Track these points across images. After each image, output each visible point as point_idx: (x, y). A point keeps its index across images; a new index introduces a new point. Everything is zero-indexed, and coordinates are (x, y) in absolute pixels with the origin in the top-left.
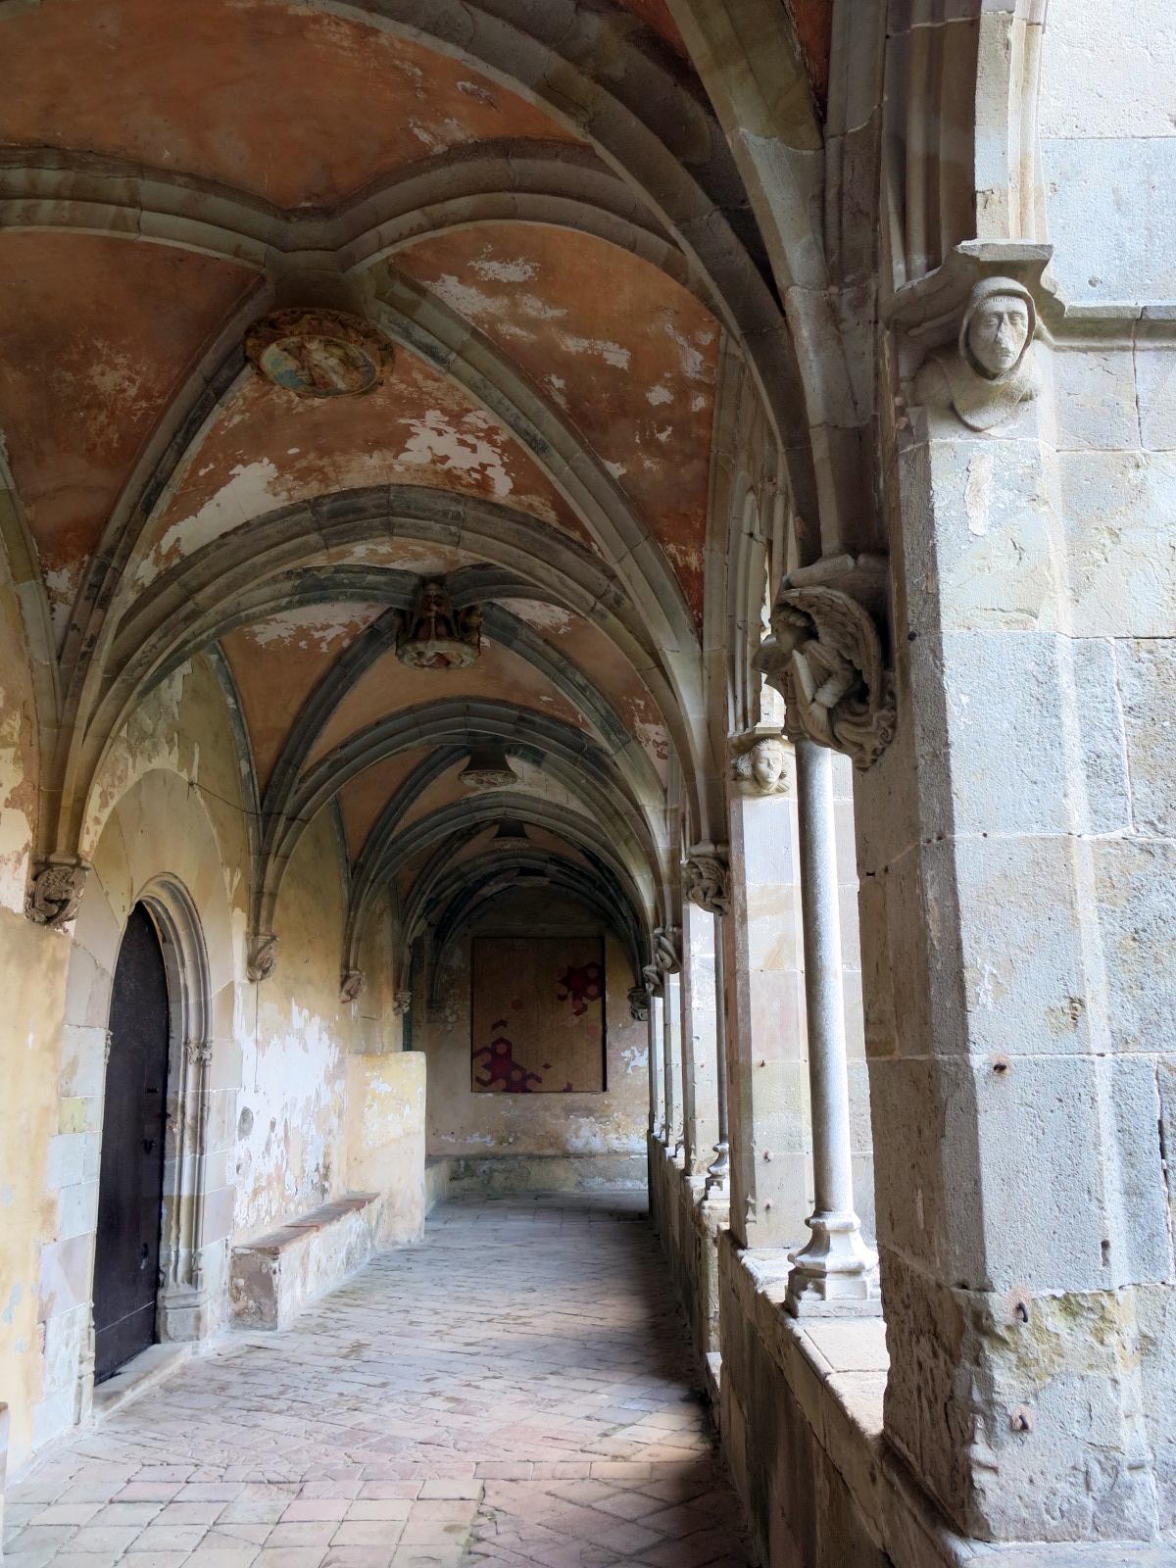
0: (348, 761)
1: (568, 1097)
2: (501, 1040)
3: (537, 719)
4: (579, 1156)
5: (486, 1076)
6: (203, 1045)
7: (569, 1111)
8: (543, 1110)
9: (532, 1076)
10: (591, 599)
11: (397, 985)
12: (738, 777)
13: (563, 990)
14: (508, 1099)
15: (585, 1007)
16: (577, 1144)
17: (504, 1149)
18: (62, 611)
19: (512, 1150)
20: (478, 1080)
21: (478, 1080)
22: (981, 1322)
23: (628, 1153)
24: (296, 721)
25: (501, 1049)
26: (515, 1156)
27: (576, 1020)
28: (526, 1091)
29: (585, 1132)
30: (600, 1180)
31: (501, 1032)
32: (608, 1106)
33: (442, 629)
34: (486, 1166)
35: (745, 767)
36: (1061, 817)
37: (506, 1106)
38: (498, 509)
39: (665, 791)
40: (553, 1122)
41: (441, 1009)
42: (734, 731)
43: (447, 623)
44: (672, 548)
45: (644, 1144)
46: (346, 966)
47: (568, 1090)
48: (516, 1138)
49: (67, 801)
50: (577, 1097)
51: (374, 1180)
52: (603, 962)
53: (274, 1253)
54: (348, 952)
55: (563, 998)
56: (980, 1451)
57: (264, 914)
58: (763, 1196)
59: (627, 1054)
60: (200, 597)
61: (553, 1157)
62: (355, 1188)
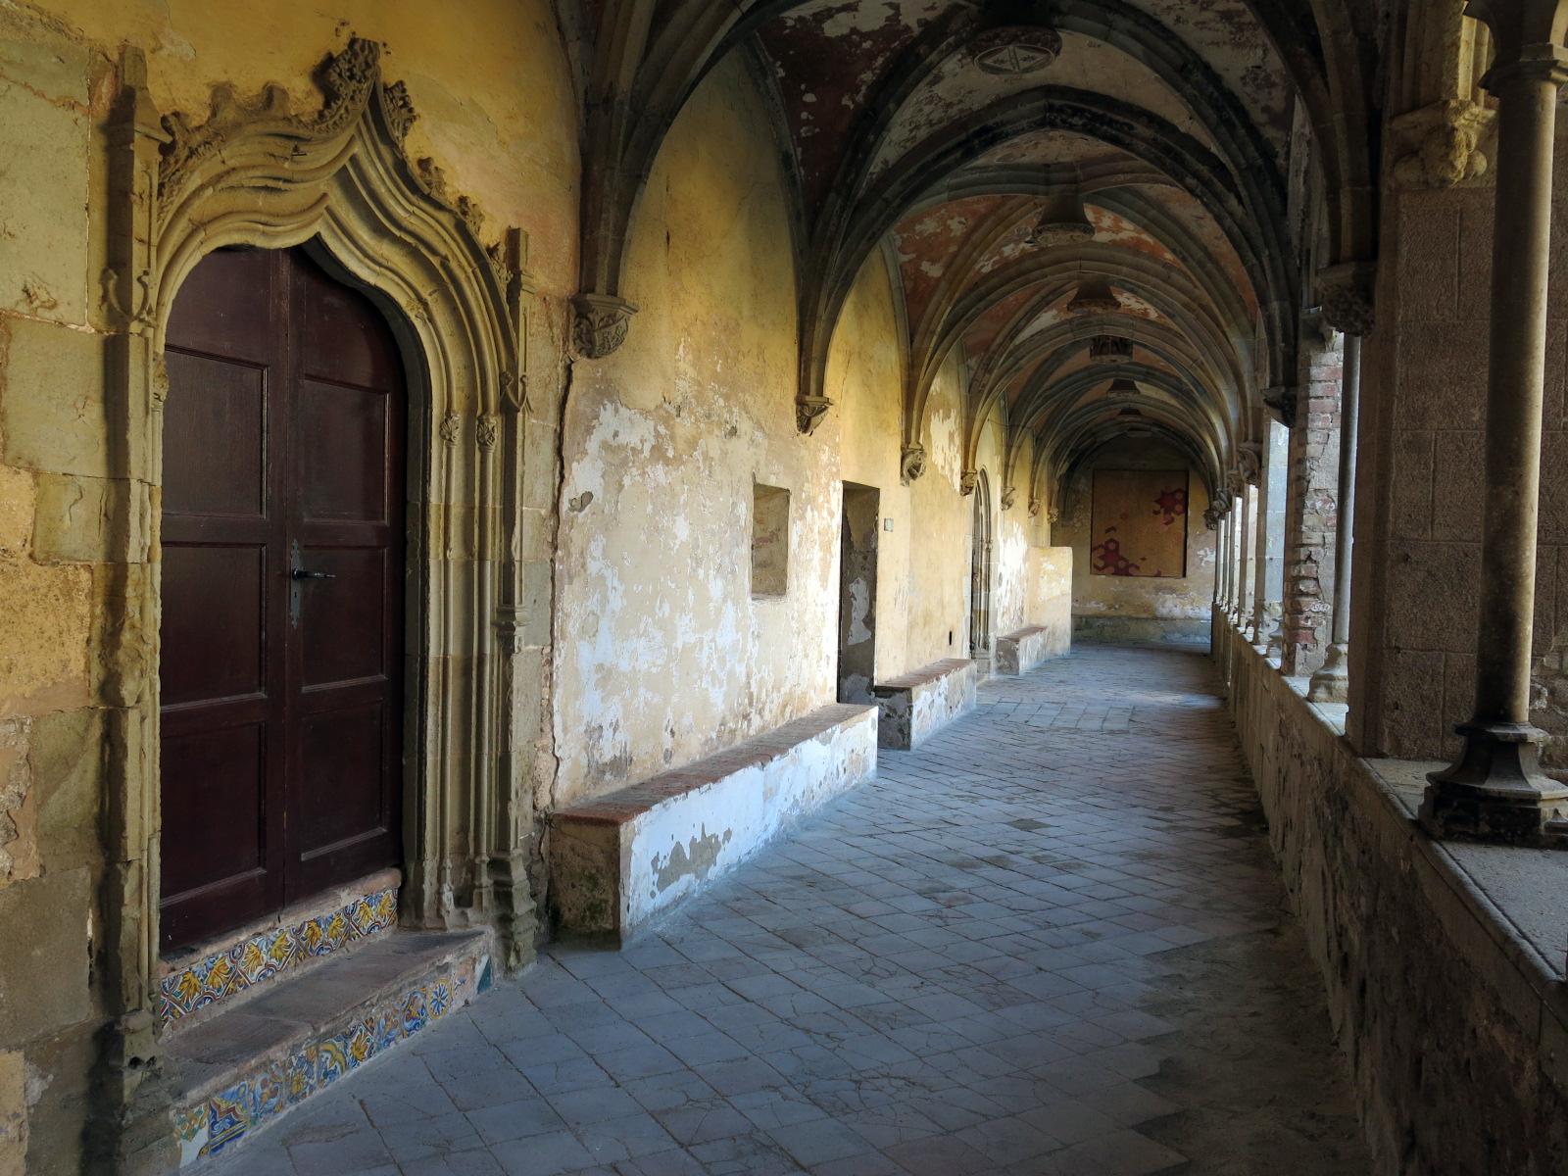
0: (1053, 396)
1: (1158, 580)
2: (1112, 540)
3: (1157, 373)
4: (1165, 619)
5: (1101, 564)
6: (989, 542)
7: (1158, 589)
8: (1141, 588)
9: (1132, 565)
11: (1050, 505)
13: (1157, 507)
14: (1116, 580)
15: (1173, 520)
16: (1164, 611)
17: (1112, 613)
18: (972, 373)
19: (1119, 613)
20: (1095, 566)
21: (1095, 566)
23: (1198, 619)
24: (1029, 380)
25: (1112, 546)
26: (1119, 617)
27: (1166, 528)
28: (1128, 574)
29: (1169, 604)
30: (1178, 635)
31: (1112, 535)
32: (1187, 587)
33: (1115, 349)
34: (1101, 621)
37: (1113, 584)
38: (1150, 322)
40: (1147, 596)
41: (1071, 518)
43: (1117, 344)
45: (1208, 614)
46: (1031, 496)
47: (1158, 575)
48: (1121, 606)
49: (971, 449)
50: (1165, 580)
51: (1044, 620)
52: (1187, 488)
53: (1017, 641)
54: (1032, 489)
55: (1156, 513)
57: (1009, 476)
59: (1202, 552)
60: (1022, 362)
61: (1147, 619)
62: (1034, 623)
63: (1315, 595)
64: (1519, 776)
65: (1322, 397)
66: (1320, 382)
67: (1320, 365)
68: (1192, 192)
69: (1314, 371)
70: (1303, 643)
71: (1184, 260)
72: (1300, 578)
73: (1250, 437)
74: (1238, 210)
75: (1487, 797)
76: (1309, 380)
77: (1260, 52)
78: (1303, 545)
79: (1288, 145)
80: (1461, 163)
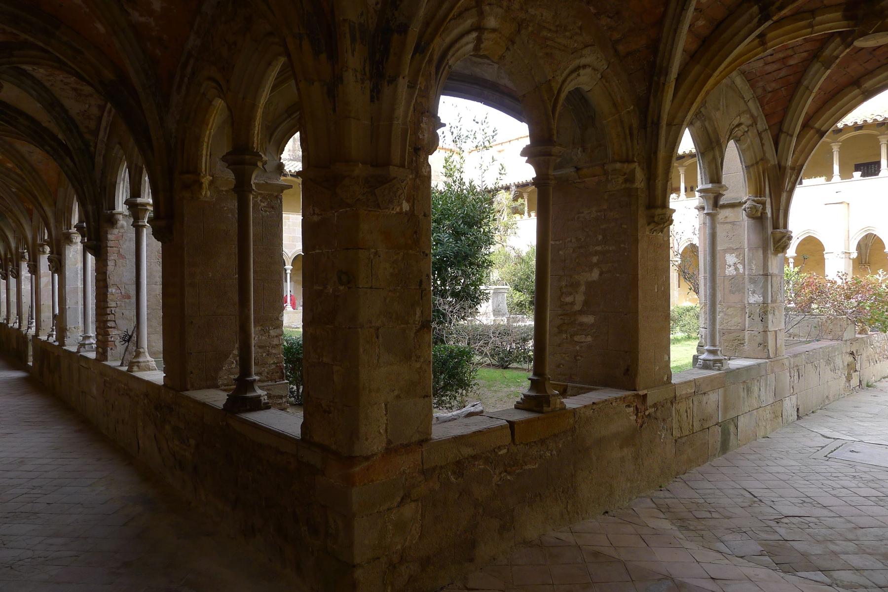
10: (5, 209)
12: (39, 251)
22: (66, 329)
35: (41, 250)
36: (77, 285)
39: (15, 232)
42: (39, 242)
44: (26, 204)
56: (65, 339)
58: (43, 327)
63: (114, 328)
64: (254, 391)
65: (113, 247)
66: (112, 241)
67: (111, 234)
68: (48, 153)
69: (109, 236)
70: (111, 347)
71: (21, 170)
72: (107, 321)
73: (55, 252)
74: (72, 164)
75: (248, 398)
76: (107, 239)
77: (87, 106)
78: (109, 307)
79: (96, 144)
80: (203, 194)
